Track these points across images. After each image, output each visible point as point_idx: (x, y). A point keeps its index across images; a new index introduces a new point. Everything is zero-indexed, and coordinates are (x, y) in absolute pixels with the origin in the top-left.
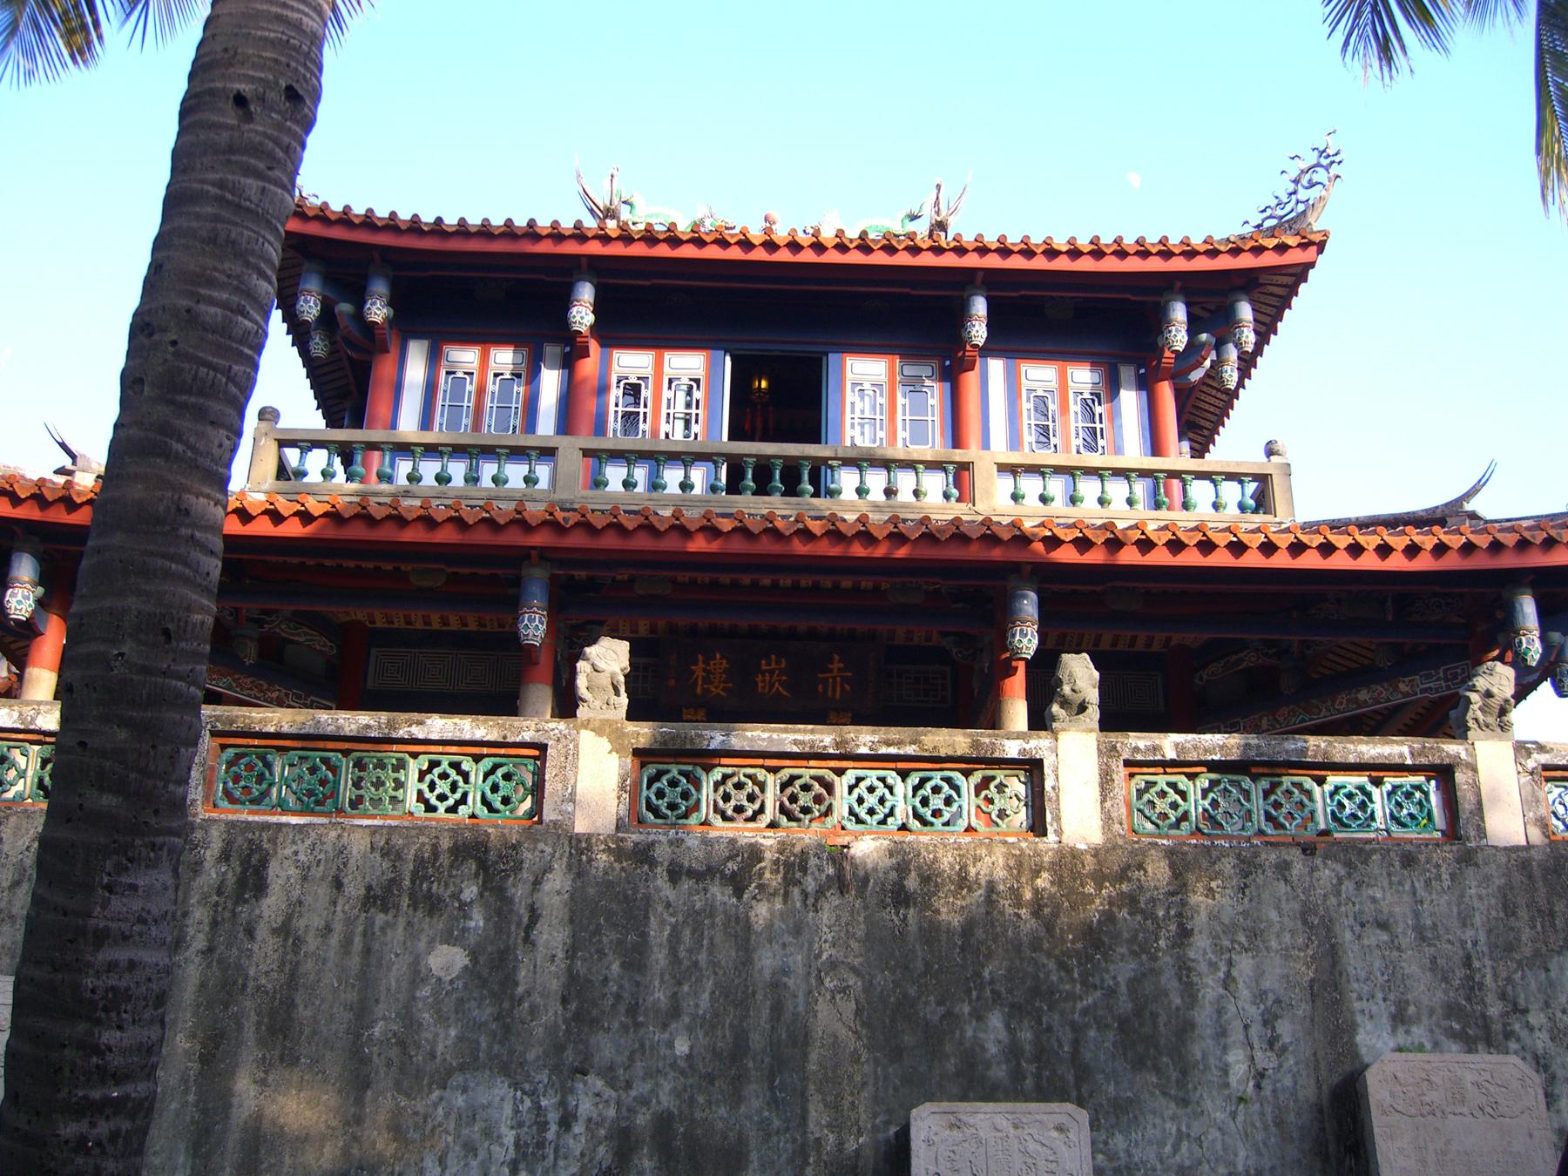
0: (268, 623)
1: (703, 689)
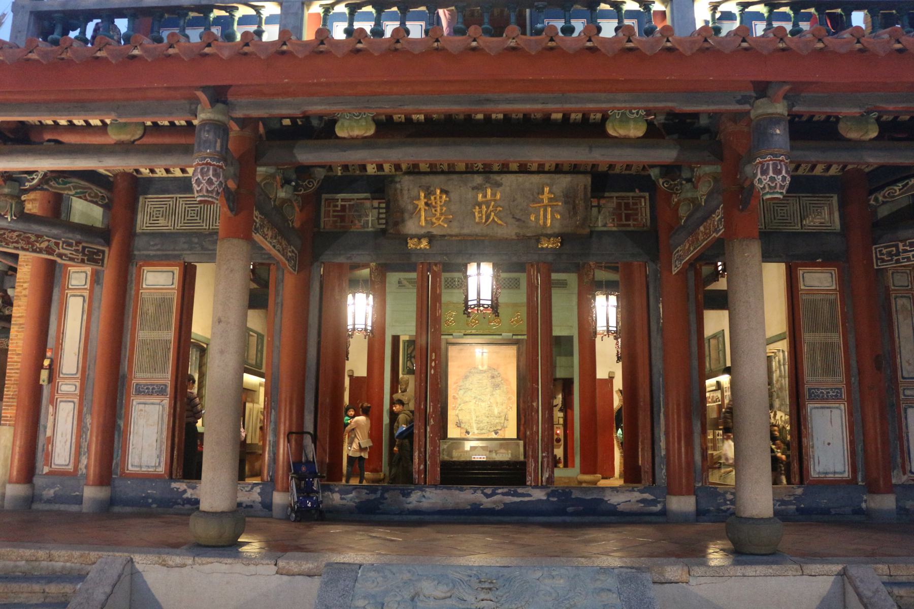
0: (29, 181)
1: (426, 220)
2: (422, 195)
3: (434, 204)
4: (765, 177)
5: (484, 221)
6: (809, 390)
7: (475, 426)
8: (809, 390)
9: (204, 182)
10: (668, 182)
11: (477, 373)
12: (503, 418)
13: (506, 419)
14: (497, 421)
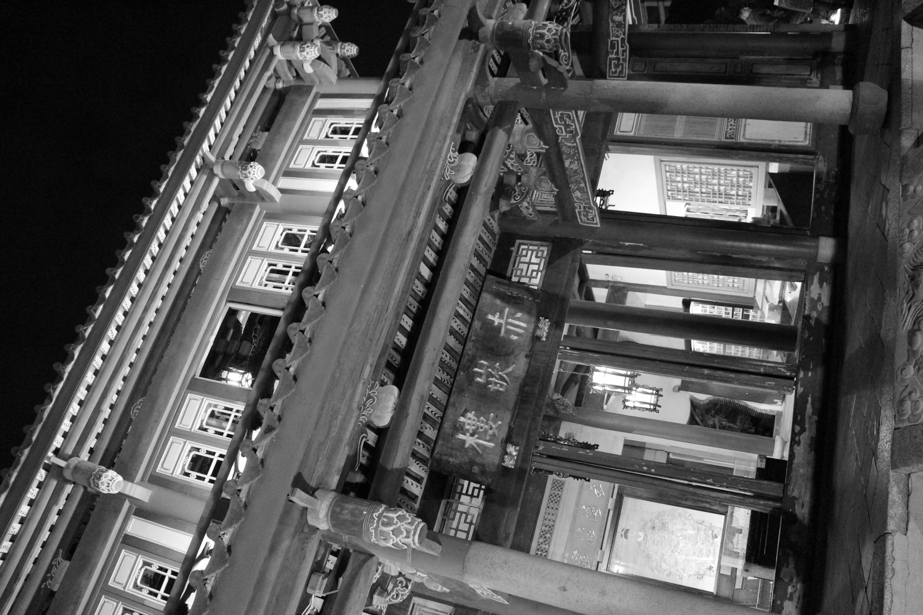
1: (488, 441)
2: (461, 436)
3: (474, 427)
4: (546, 36)
5: (505, 384)
6: (726, 138)
7: (704, 559)
8: (726, 138)
9: (398, 525)
10: (515, 196)
11: (645, 544)
12: (700, 526)
13: (702, 523)
14: (702, 533)
